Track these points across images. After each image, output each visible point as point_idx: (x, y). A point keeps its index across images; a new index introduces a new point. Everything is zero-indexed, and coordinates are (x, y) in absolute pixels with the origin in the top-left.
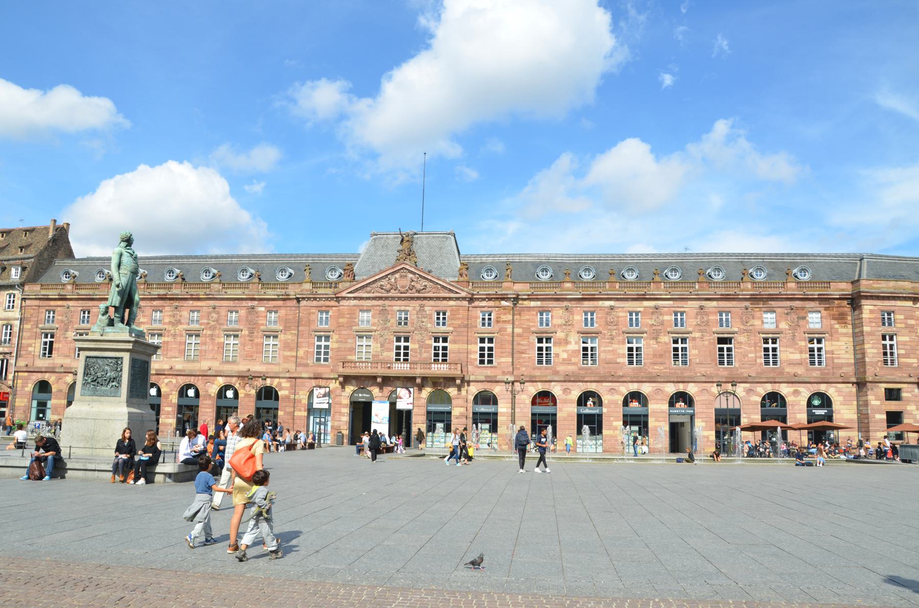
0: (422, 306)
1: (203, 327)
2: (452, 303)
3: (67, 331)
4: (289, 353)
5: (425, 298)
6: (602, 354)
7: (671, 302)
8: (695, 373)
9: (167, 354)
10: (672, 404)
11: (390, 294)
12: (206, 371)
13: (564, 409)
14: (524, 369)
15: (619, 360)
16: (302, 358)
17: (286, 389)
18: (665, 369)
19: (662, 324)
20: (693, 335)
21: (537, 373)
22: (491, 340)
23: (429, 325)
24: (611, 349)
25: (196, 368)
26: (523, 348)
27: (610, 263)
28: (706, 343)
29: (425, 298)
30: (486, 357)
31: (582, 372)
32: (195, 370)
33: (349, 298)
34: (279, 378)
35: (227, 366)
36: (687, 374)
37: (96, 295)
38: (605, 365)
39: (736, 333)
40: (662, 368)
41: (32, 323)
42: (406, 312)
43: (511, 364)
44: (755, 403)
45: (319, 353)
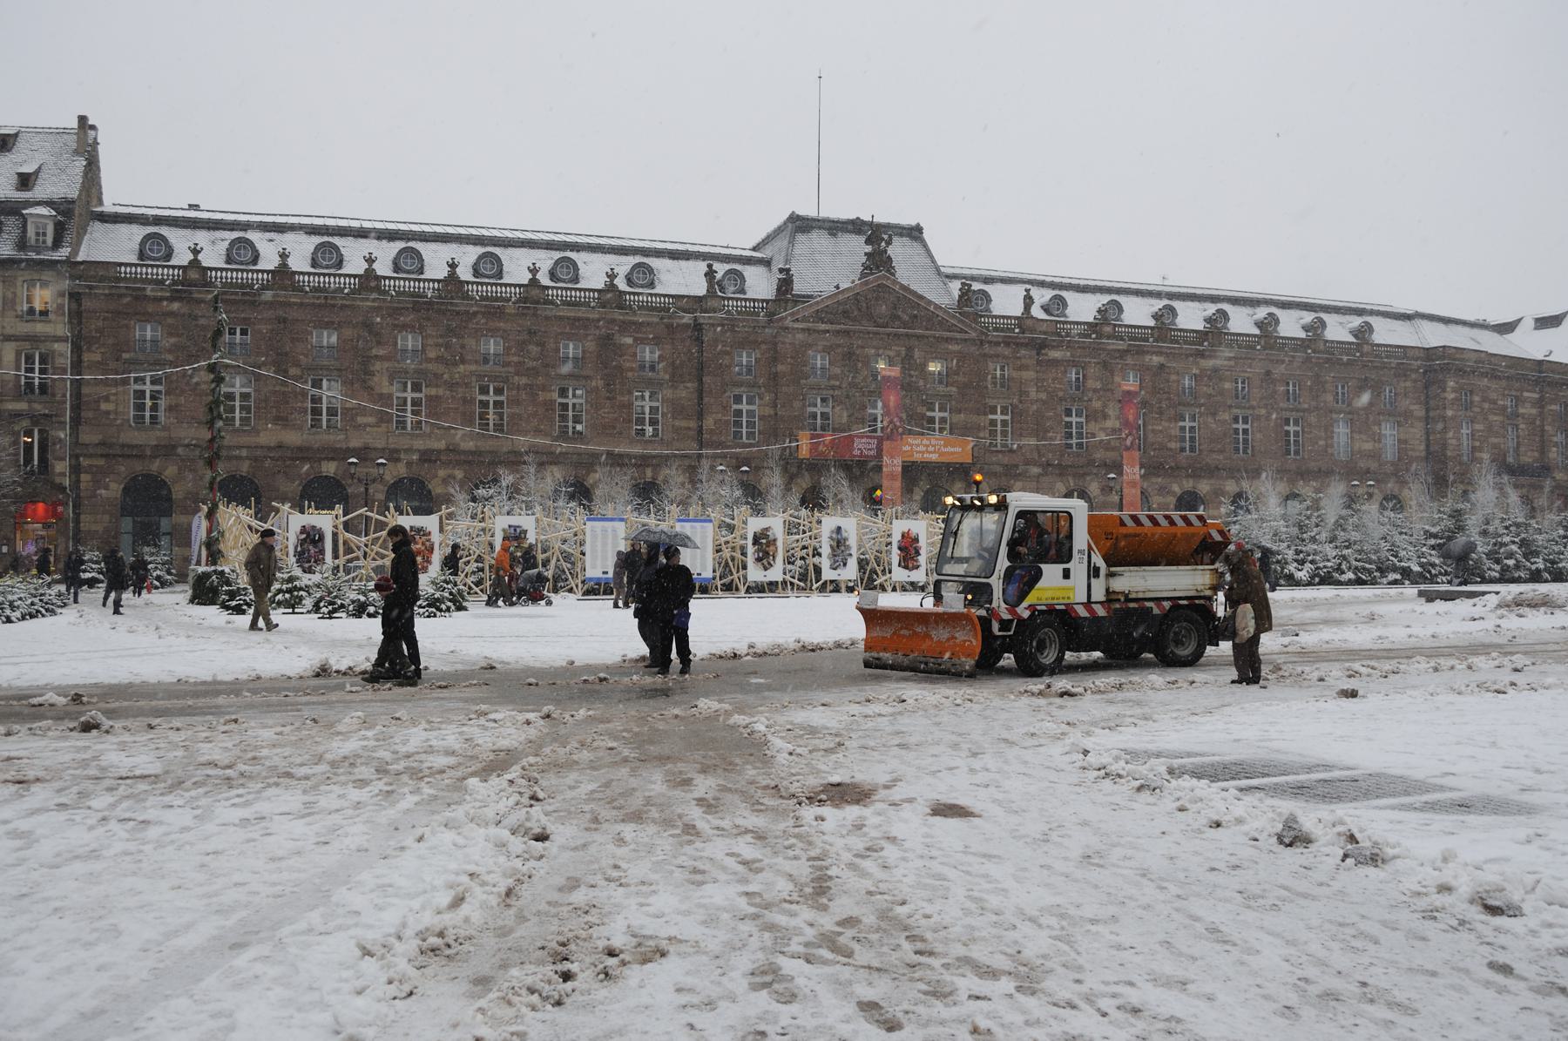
0: (910, 349)
4: (684, 424)
6: (1150, 436)
15: (1169, 445)
16: (711, 432)
19: (1222, 393)
23: (921, 383)
39: (1304, 411)
45: (738, 424)
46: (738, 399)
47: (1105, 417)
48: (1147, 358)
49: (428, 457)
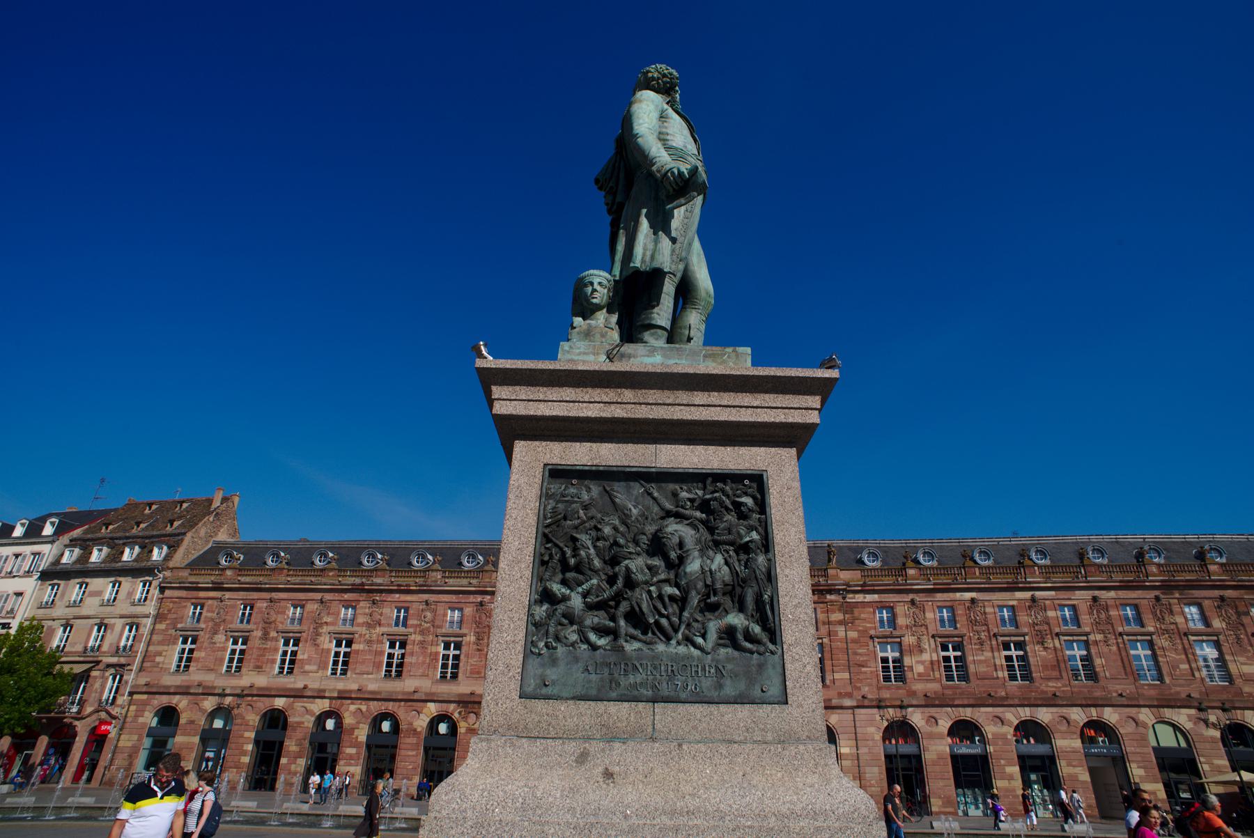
1: (411, 630)
3: (216, 633)
6: (972, 668)
7: (1053, 593)
8: (1110, 692)
9: (355, 669)
10: (1088, 741)
12: (409, 693)
13: (932, 748)
14: (867, 689)
18: (1063, 686)
19: (1047, 622)
20: (1092, 637)
21: (886, 694)
24: (983, 658)
25: (398, 689)
26: (861, 659)
27: (947, 546)
28: (1114, 648)
31: (948, 692)
32: (396, 692)
35: (443, 687)
36: (1098, 693)
37: (266, 584)
38: (978, 682)
40: (1060, 685)
41: (168, 622)
43: (849, 681)
47: (921, 651)
48: (958, 595)
49: (343, 696)
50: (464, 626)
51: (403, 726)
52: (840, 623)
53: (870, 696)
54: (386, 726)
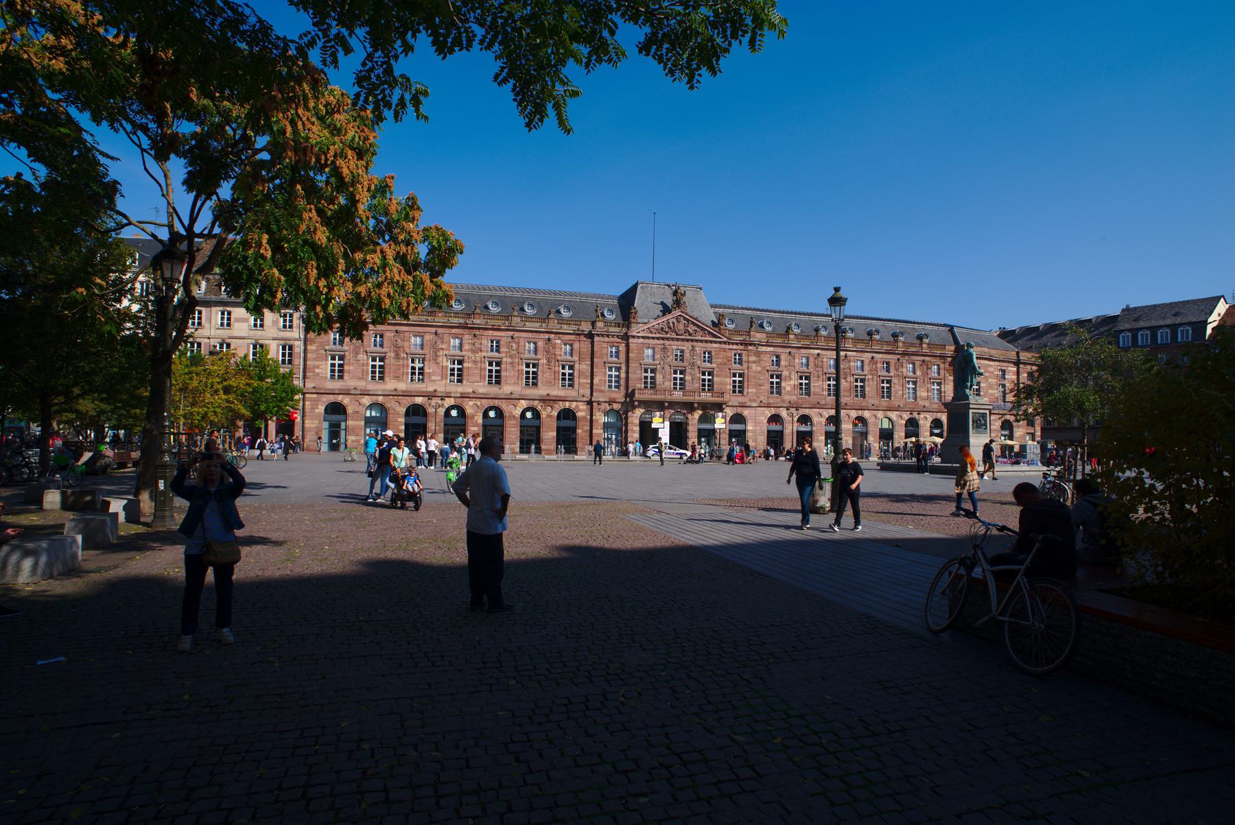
1: (503, 355)
2: (715, 345)
4: (584, 381)
5: (697, 341)
10: (855, 425)
11: (668, 336)
12: (508, 395)
16: (598, 385)
17: (583, 411)
20: (867, 377)
21: (771, 401)
22: (740, 375)
29: (697, 341)
30: (739, 388)
31: (800, 401)
33: (639, 337)
34: (577, 401)
42: (682, 351)
44: (902, 425)
46: (610, 369)
47: (790, 379)
50: (538, 353)
51: (506, 414)
52: (754, 362)
53: (764, 401)
54: (492, 414)
